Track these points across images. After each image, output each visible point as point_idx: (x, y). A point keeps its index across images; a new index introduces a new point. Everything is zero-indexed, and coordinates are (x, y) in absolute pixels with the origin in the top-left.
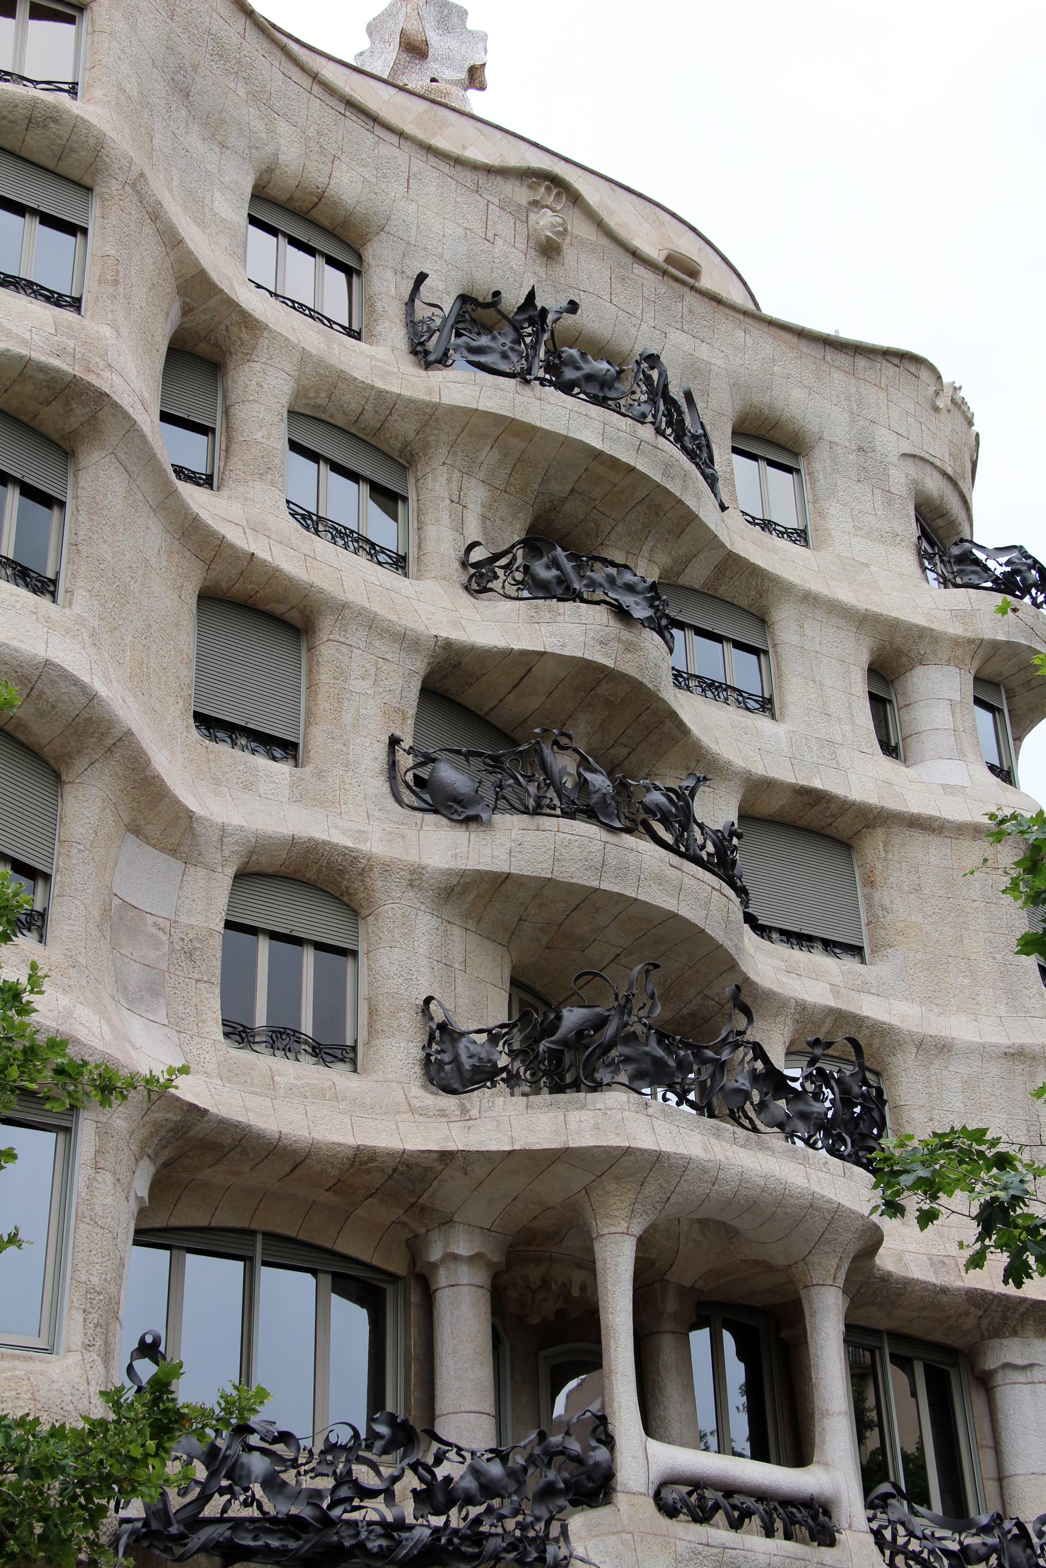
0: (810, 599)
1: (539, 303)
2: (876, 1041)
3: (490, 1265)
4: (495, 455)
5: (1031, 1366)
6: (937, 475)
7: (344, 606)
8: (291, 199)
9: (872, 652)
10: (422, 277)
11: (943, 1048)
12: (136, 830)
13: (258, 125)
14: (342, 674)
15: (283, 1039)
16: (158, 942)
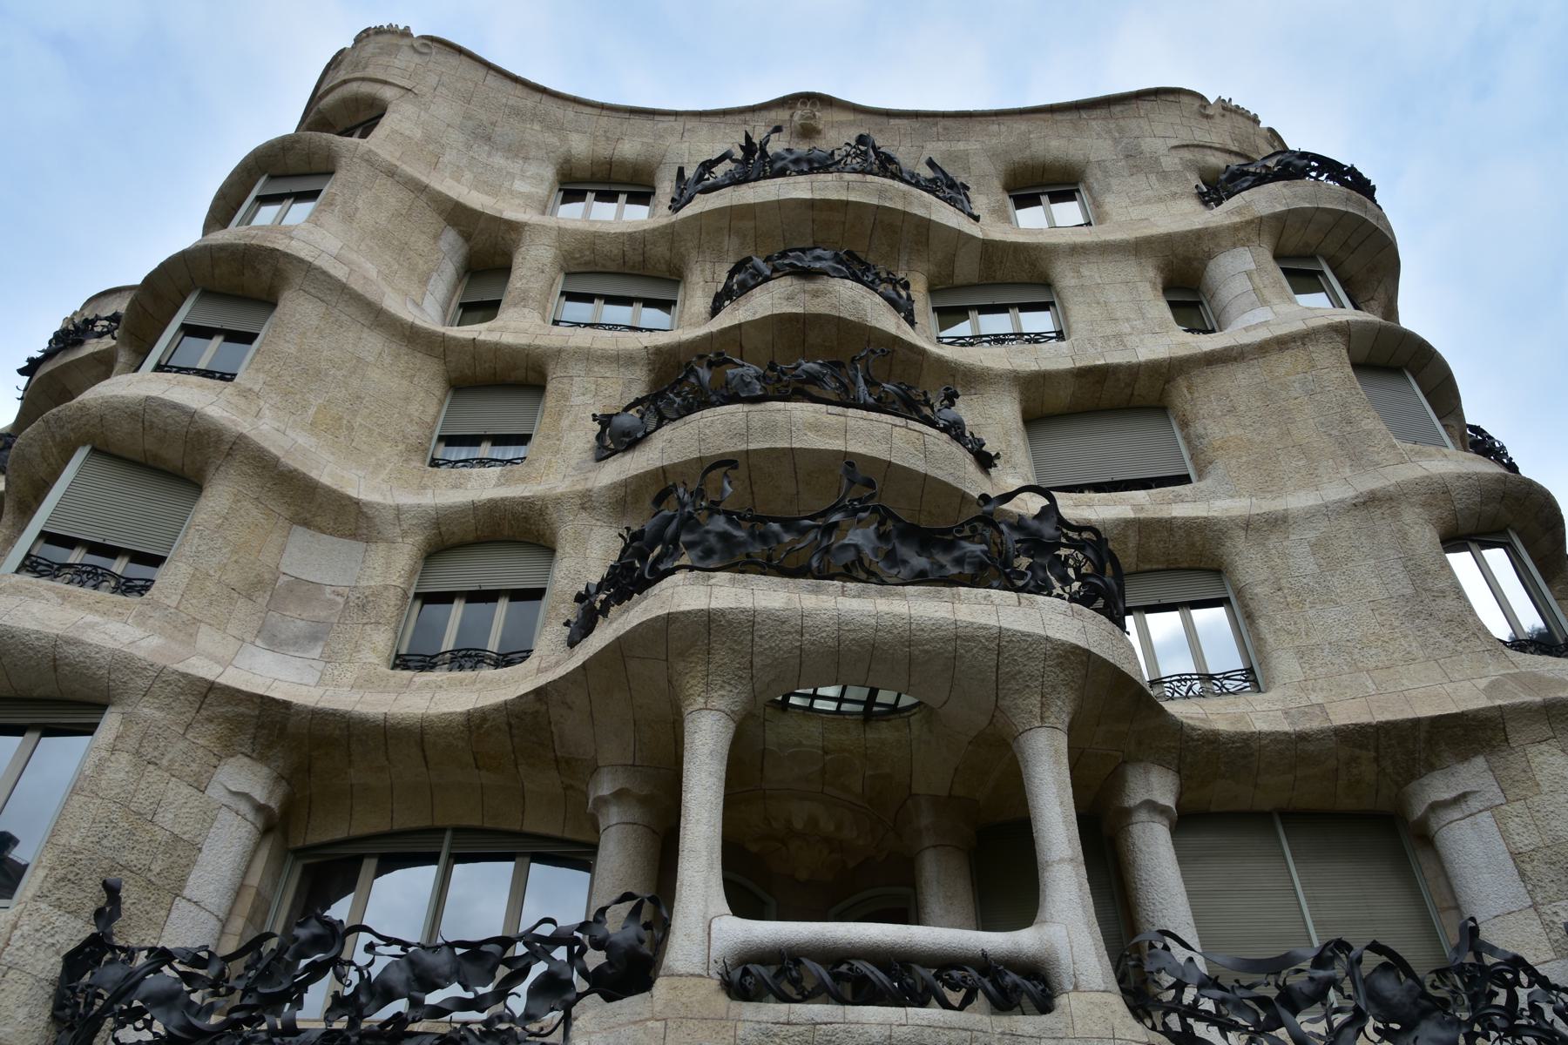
0: (1078, 251)
1: (756, 140)
2: (1197, 538)
3: (644, 801)
4: (735, 241)
5: (1463, 797)
6: (1218, 154)
7: (560, 351)
8: (593, 174)
9: (1160, 269)
10: (681, 171)
11: (1278, 522)
12: (306, 524)
13: (555, 141)
14: (565, 397)
15: (468, 657)
16: (333, 604)
